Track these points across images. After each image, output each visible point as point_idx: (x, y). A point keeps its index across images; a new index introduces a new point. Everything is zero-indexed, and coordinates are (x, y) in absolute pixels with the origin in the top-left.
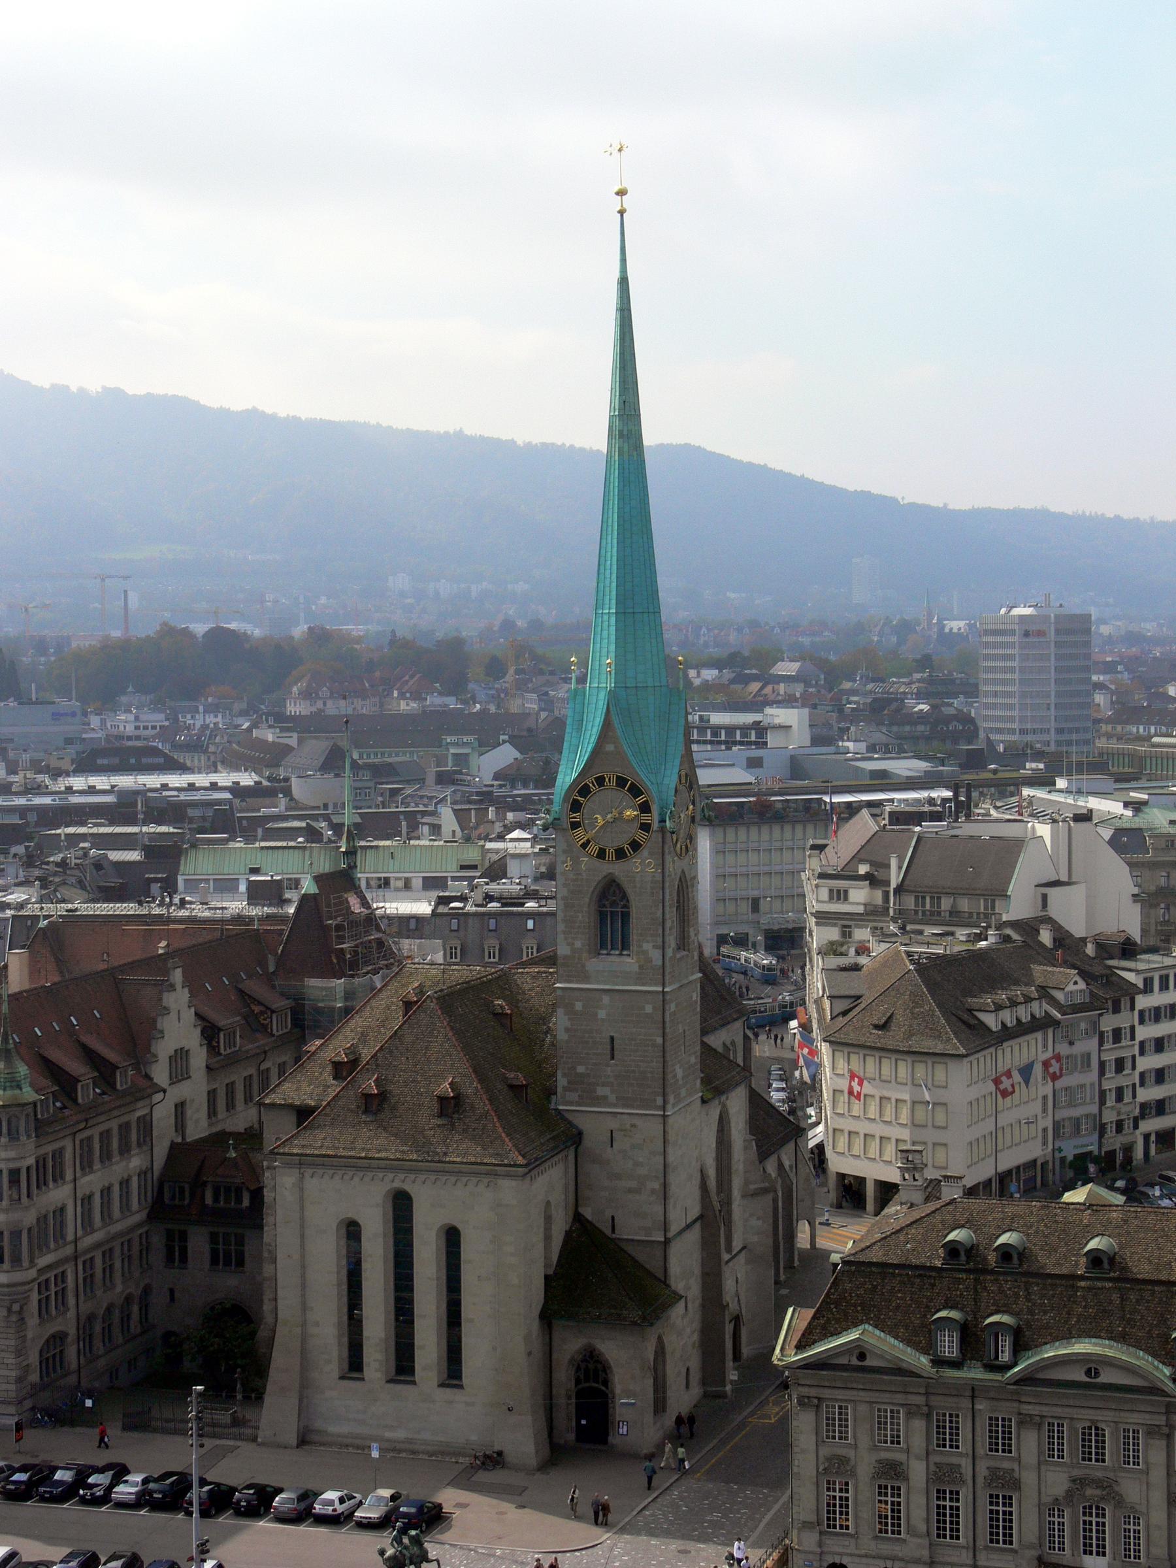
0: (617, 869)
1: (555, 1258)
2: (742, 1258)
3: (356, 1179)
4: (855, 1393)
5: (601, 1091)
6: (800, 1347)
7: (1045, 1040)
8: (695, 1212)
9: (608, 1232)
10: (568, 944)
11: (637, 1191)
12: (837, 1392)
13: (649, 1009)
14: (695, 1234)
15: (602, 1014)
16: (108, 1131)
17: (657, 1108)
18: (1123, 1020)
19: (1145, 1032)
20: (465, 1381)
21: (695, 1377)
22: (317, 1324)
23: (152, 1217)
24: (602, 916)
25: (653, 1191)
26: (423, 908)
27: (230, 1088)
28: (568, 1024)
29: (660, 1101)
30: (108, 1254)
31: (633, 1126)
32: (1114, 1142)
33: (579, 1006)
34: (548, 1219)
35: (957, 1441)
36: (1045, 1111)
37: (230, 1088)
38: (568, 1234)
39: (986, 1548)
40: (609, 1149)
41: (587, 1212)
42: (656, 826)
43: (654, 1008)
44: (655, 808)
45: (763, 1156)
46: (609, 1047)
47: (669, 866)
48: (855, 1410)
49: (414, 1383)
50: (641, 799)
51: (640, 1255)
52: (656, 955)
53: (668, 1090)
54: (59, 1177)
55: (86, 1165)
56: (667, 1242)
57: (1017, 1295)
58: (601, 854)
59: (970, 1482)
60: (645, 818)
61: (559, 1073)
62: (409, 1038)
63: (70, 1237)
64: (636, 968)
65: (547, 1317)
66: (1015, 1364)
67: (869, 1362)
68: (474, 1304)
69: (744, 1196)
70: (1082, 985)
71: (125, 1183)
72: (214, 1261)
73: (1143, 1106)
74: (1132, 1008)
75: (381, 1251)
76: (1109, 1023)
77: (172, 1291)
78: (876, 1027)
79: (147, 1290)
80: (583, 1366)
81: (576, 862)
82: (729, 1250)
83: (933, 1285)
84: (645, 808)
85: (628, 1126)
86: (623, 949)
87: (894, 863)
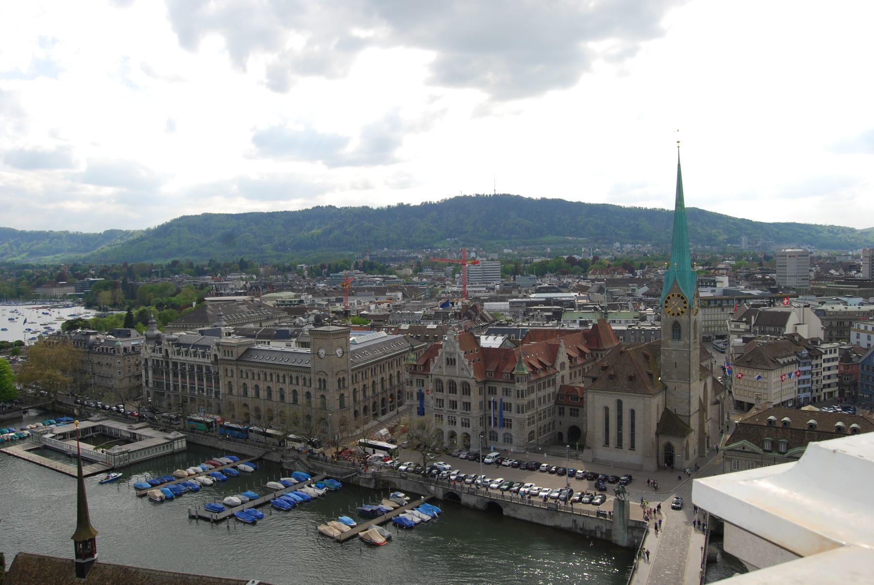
1: (660, 418)
2: (710, 421)
5: (672, 376)
6: (726, 445)
7: (796, 366)
8: (697, 408)
9: (674, 412)
13: (686, 355)
14: (697, 415)
15: (673, 356)
16: (545, 382)
18: (819, 361)
19: (824, 365)
20: (635, 449)
21: (697, 452)
23: (556, 404)
24: (673, 330)
26: (625, 328)
27: (575, 372)
29: (688, 379)
30: (545, 412)
32: (815, 395)
33: (667, 354)
34: (658, 409)
36: (795, 385)
37: (575, 372)
38: (663, 413)
41: (668, 407)
42: (688, 307)
45: (716, 394)
47: (692, 318)
50: (684, 300)
51: (682, 418)
52: (688, 341)
53: (691, 376)
54: (533, 392)
55: (540, 390)
56: (690, 416)
57: (788, 434)
60: (685, 305)
63: (536, 407)
65: (657, 434)
67: (746, 450)
69: (711, 405)
70: (807, 352)
71: (549, 395)
72: (571, 414)
73: (824, 385)
74: (821, 358)
76: (814, 362)
77: (560, 422)
78: (748, 362)
79: (554, 422)
81: (666, 316)
82: (706, 419)
84: (685, 302)
87: (753, 318)
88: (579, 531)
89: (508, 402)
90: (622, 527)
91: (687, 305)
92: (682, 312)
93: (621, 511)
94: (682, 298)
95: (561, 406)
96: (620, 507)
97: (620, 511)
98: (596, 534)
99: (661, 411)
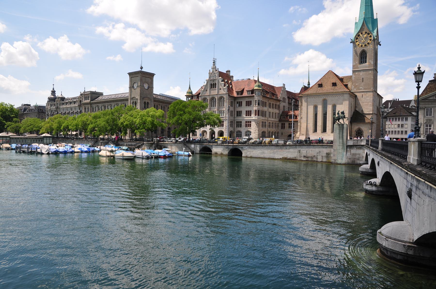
3: (317, 98)
4: (434, 105)
5: (360, 88)
9: (361, 113)
11: (367, 105)
12: (429, 105)
22: (309, 124)
25: (370, 104)
28: (355, 77)
29: (372, 88)
34: (351, 107)
41: (357, 109)
44: (372, 36)
48: (434, 109)
50: (370, 35)
62: (326, 76)
64: (368, 65)
77: (282, 133)
78: (394, 113)
80: (358, 132)
87: (389, 104)
88: (302, 159)
89: (249, 110)
90: (341, 147)
91: (372, 38)
92: (368, 43)
93: (341, 133)
95: (283, 123)
96: (339, 130)
97: (339, 134)
99: (353, 110)
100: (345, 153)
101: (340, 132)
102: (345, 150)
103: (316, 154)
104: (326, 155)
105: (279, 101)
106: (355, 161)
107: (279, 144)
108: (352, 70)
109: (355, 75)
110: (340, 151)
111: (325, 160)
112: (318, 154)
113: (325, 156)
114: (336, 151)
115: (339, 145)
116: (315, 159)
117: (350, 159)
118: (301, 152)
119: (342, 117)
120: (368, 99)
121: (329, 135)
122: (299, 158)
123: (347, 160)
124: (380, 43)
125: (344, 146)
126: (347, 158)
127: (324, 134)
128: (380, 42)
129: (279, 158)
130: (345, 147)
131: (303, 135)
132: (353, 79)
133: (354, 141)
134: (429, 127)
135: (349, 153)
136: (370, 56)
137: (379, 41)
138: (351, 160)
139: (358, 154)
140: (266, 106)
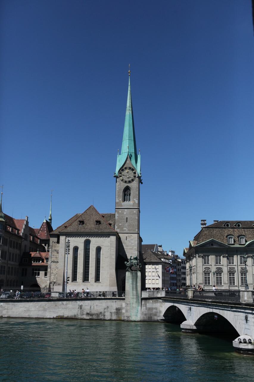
0: (129, 185)
5: (124, 229)
10: (118, 200)
11: (132, 249)
13: (135, 212)
15: (125, 213)
17: (136, 232)
25: (135, 249)
31: (131, 235)
33: (120, 212)
35: (233, 262)
39: (240, 286)
40: (126, 241)
43: (136, 212)
46: (126, 220)
49: (89, 282)
50: (134, 171)
58: (126, 182)
59: (237, 271)
61: (116, 225)
64: (132, 204)
66: (246, 244)
68: (104, 263)
75: (83, 253)
81: (120, 183)
83: (224, 231)
84: (135, 173)
85: (130, 236)
86: (129, 201)
90: (135, 300)
93: (135, 283)
94: (133, 170)
96: (133, 279)
97: (133, 284)
98: (104, 315)
100: (140, 307)
101: (133, 281)
102: (140, 305)
103: (102, 311)
104: (115, 311)
105: (20, 237)
106: (151, 317)
107: (52, 297)
108: (115, 207)
109: (118, 213)
110: (134, 305)
111: (114, 317)
112: (106, 310)
113: (115, 312)
114: (128, 306)
115: (133, 298)
116: (101, 317)
117: (146, 314)
118: (83, 308)
119: (135, 264)
120: (133, 242)
121: (92, 285)
122: (80, 317)
123: (142, 316)
124: (142, 181)
125: (138, 299)
126: (142, 313)
127: (86, 283)
128: (141, 180)
129: (52, 317)
130: (140, 300)
131: (59, 284)
132: (116, 218)
133: (150, 293)
134: (208, 275)
135: (145, 307)
136: (134, 192)
137: (141, 179)
138: (147, 316)
139: (155, 309)
140: (6, 245)
